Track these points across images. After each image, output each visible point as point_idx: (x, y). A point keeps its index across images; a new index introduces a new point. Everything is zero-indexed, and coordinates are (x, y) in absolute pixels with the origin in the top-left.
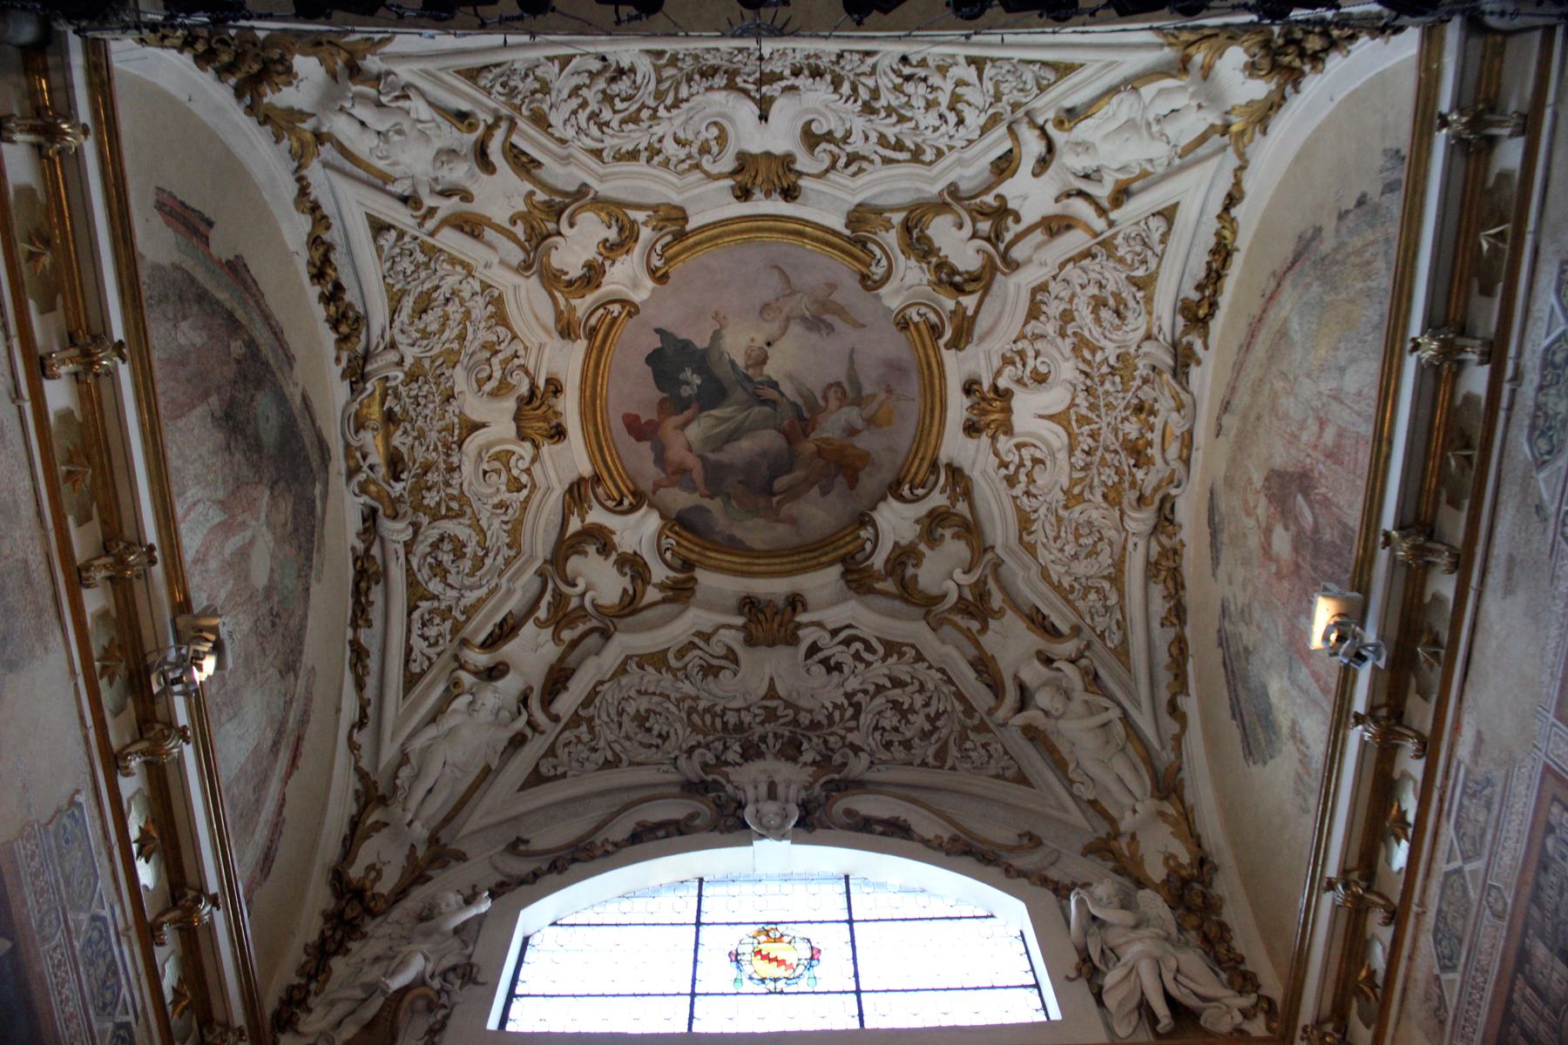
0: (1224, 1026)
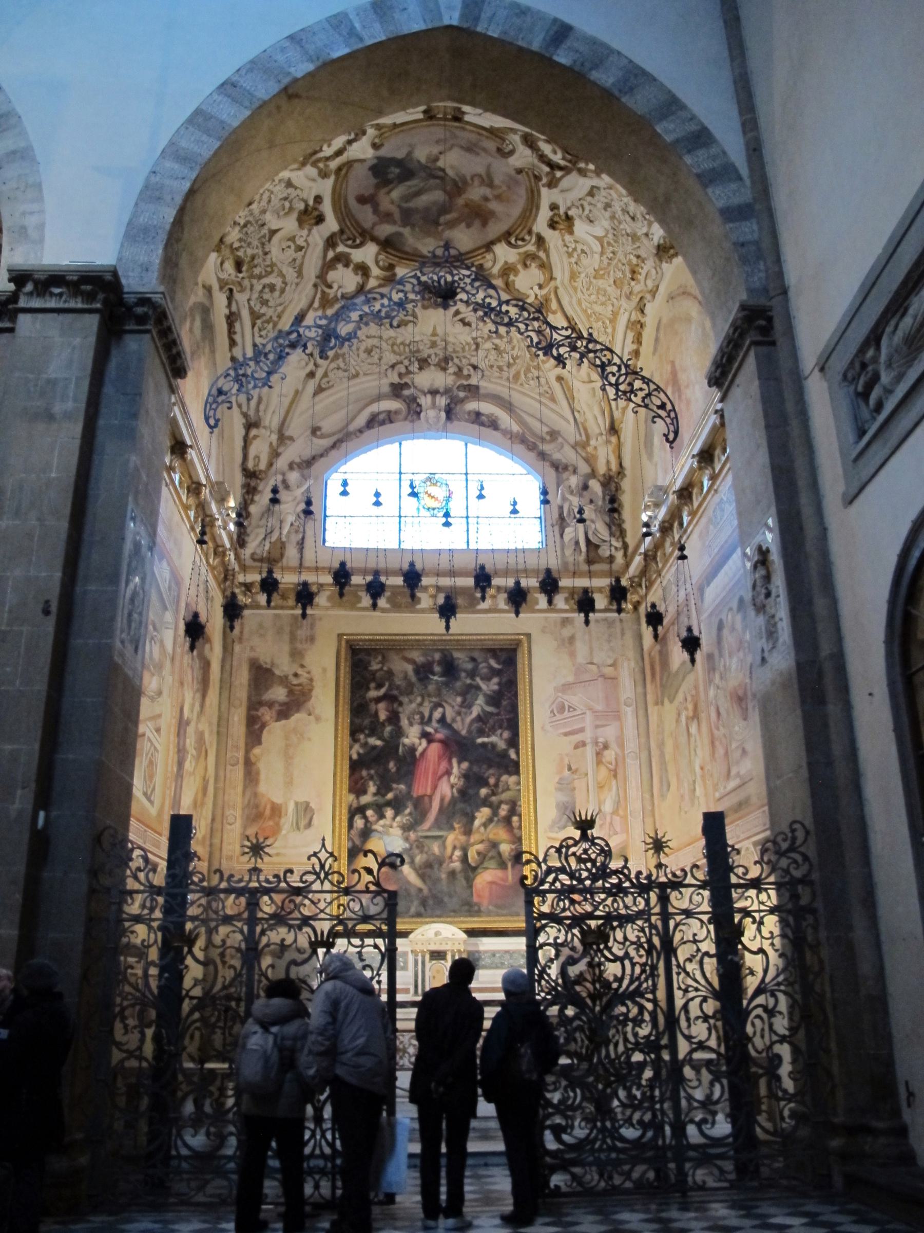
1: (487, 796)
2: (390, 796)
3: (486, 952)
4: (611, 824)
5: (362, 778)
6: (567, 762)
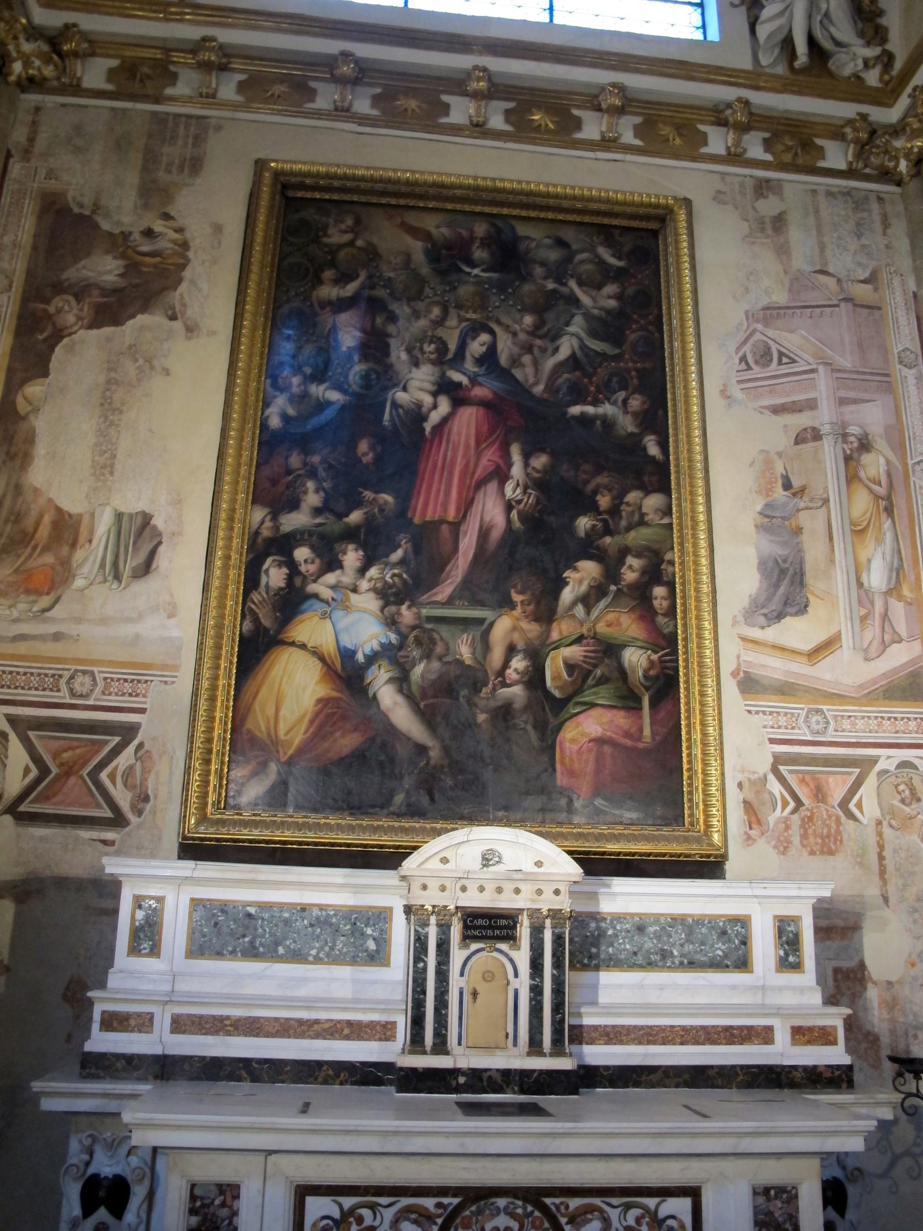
0: (847, 71)
1: (592, 534)
2: (355, 517)
3: (619, 918)
4: (885, 616)
5: (289, 472)
6: (779, 469)
